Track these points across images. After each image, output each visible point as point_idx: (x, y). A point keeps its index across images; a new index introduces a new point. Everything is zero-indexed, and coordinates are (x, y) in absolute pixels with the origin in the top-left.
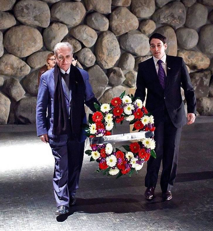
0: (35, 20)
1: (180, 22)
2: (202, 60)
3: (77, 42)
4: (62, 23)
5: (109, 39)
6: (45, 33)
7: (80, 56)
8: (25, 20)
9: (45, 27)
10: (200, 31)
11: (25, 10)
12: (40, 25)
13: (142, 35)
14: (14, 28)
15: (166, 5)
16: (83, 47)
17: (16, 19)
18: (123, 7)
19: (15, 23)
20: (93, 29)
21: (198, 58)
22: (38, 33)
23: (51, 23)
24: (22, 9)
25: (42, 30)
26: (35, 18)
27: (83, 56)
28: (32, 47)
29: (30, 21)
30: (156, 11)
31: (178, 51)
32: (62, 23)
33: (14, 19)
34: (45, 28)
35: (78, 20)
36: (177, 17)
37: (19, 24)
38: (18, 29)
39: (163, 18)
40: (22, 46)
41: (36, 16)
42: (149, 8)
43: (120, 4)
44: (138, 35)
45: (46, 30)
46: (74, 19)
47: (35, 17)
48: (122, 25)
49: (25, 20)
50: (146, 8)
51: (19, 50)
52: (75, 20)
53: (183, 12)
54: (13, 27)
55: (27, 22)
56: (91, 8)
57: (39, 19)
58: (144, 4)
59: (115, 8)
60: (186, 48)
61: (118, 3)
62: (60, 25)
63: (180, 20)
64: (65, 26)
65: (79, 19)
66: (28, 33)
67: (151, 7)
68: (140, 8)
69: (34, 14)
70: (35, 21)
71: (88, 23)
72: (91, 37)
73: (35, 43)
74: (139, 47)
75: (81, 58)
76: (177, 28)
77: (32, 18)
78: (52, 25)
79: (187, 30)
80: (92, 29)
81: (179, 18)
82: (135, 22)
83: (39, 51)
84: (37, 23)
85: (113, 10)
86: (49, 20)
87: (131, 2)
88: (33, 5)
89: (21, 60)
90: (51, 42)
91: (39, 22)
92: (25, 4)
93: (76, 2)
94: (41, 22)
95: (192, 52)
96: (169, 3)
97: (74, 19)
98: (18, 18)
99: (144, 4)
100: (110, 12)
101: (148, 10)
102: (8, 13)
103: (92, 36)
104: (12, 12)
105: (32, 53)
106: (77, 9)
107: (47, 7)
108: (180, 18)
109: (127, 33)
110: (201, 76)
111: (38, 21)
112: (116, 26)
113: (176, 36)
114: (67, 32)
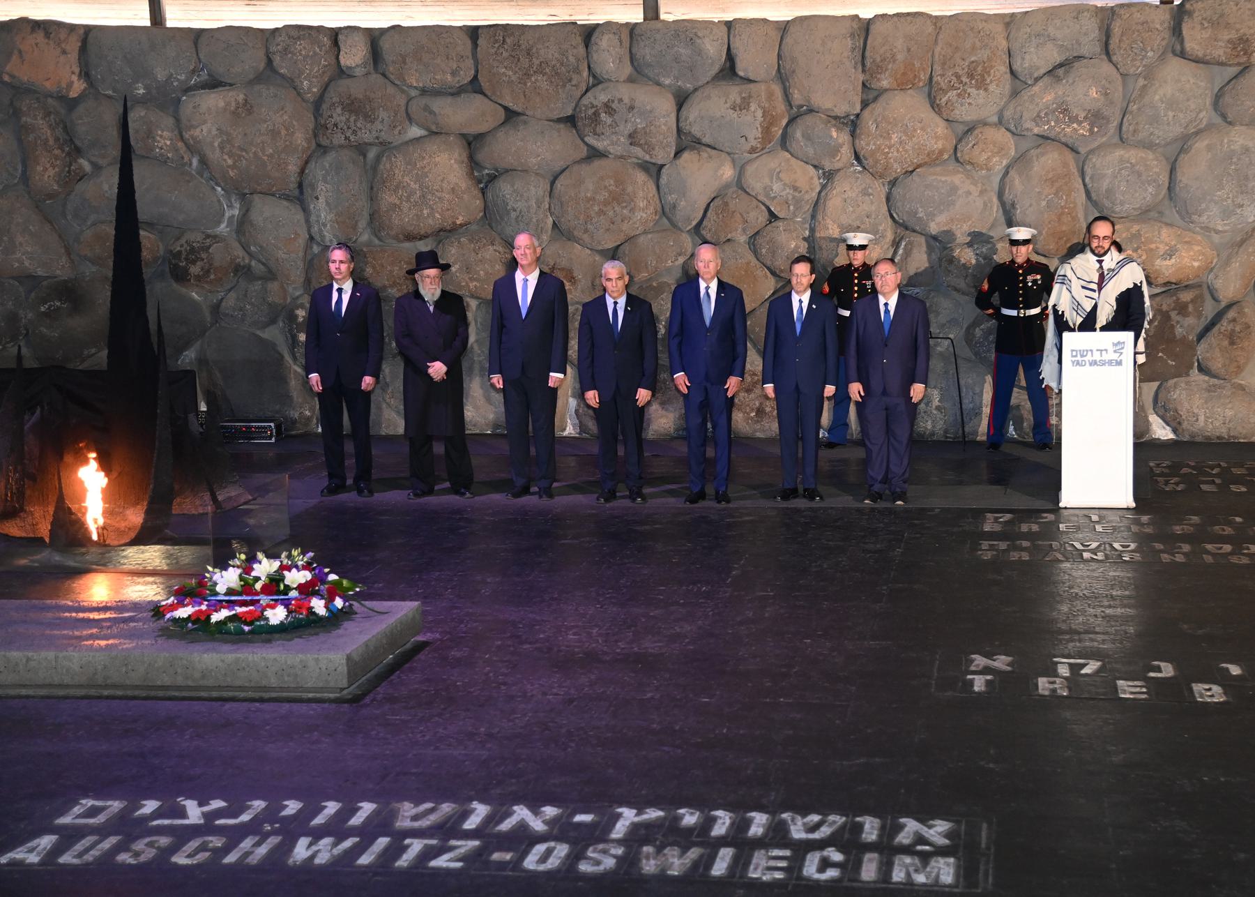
1: (1091, 131)
2: (1170, 254)
4: (709, 146)
5: (849, 194)
6: (664, 179)
12: (647, 158)
13: (957, 179)
14: (576, 167)
16: (773, 217)
21: (1153, 246)
22: (641, 177)
23: (678, 154)
24: (596, 114)
25: (654, 171)
26: (633, 138)
30: (1015, 93)
32: (709, 146)
34: (662, 166)
36: (1082, 115)
37: (595, 154)
38: (585, 169)
39: (1034, 120)
41: (635, 131)
42: (986, 90)
43: (885, 83)
45: (664, 170)
47: (630, 136)
48: (890, 148)
50: (973, 91)
51: (586, 231)
58: (964, 79)
59: (870, 95)
61: (879, 80)
63: (1092, 125)
64: (724, 155)
67: (992, 87)
69: (629, 128)
72: (796, 189)
73: (632, 210)
75: (764, 251)
77: (622, 139)
82: (935, 135)
83: (645, 232)
85: (865, 104)
86: (674, 144)
88: (626, 100)
92: (603, 98)
93: (752, 86)
94: (649, 148)
96: (1061, 65)
98: (586, 139)
99: (964, 79)
101: (977, 96)
102: (562, 126)
103: (798, 184)
104: (571, 121)
105: (622, 238)
106: (753, 107)
107: (664, 106)
108: (1096, 118)
110: (1165, 308)
111: (640, 145)
112: (873, 153)
113: (1083, 174)
114: (728, 172)
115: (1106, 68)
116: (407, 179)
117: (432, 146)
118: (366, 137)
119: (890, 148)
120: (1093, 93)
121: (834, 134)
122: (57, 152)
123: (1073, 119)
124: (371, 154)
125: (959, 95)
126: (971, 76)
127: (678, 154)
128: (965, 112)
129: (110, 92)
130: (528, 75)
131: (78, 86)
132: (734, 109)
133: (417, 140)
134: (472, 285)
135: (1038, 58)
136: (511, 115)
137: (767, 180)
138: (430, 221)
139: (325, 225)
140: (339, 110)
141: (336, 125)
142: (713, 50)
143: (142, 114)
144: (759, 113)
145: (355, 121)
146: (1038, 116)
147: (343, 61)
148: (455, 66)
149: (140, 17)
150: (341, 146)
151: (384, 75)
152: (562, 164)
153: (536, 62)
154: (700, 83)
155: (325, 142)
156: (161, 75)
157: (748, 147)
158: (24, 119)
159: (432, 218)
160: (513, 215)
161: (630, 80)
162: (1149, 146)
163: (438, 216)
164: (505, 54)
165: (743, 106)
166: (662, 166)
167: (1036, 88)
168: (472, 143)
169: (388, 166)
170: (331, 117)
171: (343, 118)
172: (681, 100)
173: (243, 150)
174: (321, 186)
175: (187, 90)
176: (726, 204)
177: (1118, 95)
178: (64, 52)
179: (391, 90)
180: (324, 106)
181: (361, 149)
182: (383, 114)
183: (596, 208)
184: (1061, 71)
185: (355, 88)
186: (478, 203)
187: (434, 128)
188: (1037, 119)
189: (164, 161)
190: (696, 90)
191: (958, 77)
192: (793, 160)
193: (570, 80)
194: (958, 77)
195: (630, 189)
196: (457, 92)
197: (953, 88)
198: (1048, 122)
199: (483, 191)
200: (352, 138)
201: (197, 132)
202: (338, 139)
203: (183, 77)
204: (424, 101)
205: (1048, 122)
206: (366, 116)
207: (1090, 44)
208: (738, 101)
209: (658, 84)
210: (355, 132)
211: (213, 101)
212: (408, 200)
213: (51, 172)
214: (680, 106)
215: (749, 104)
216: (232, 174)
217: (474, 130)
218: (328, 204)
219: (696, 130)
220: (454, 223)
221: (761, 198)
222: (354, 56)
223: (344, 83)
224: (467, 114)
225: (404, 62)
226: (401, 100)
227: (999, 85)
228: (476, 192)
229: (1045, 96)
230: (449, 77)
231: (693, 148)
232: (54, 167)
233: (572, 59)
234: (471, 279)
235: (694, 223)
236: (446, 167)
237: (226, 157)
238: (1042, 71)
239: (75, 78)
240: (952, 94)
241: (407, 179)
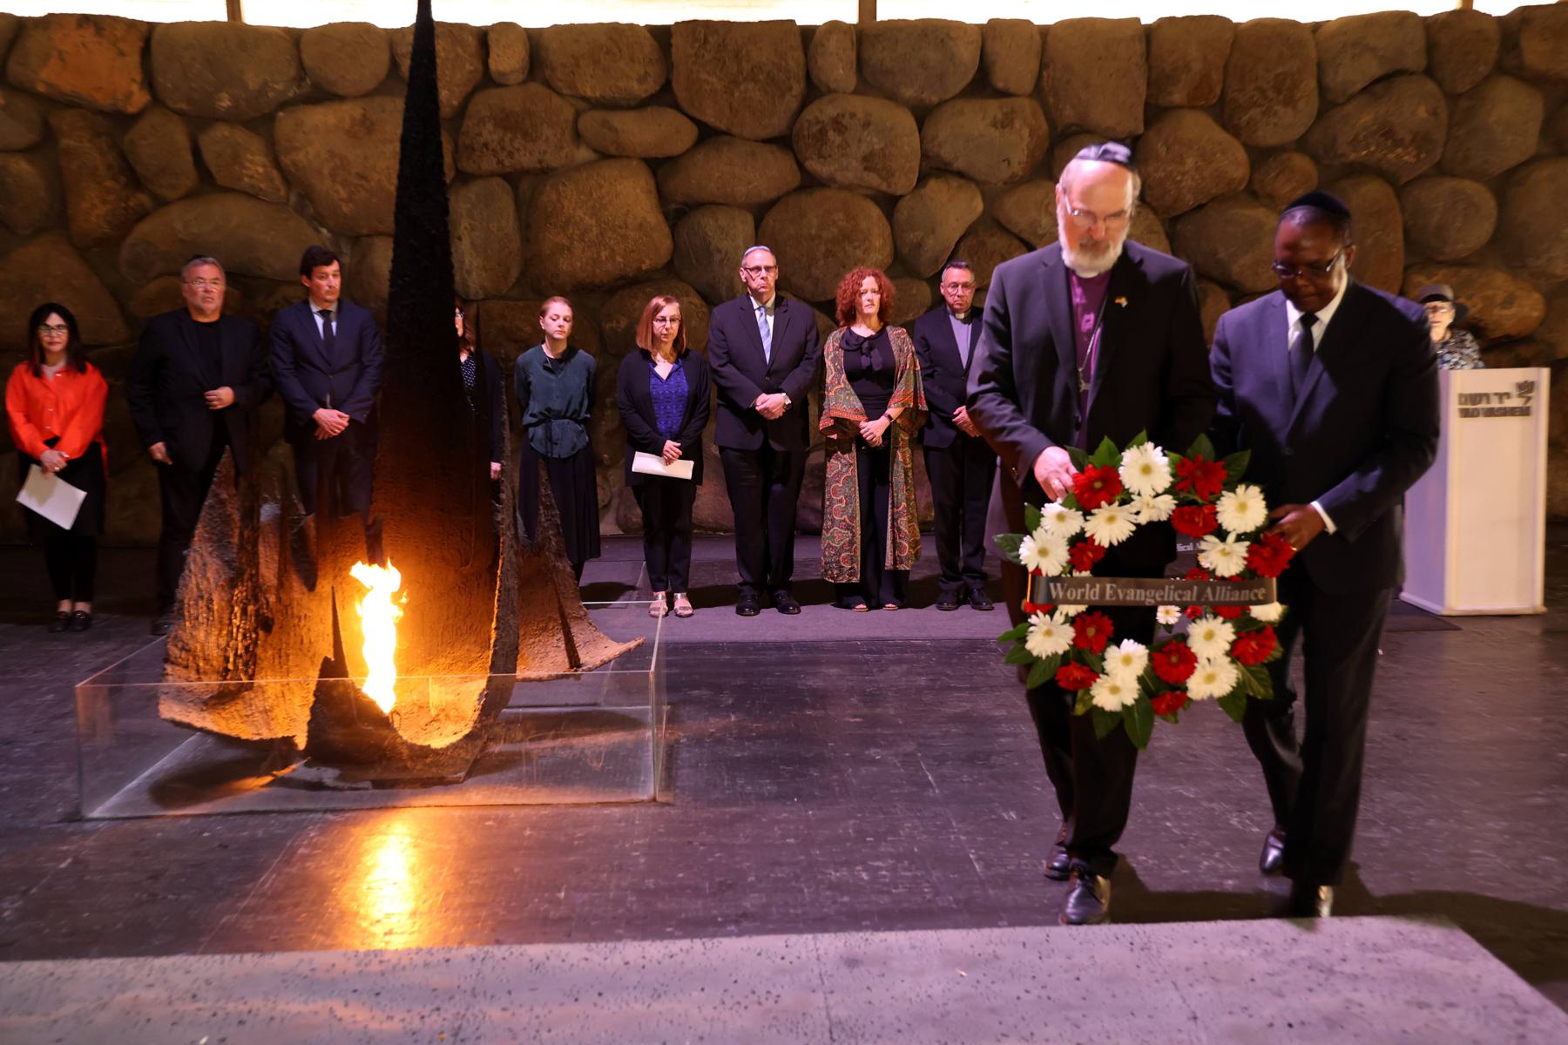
1: (1417, 156)
2: (1508, 302)
3: (1016, 243)
4: (961, 175)
9: (899, 193)
10: (1505, 184)
11: (831, 134)
12: (884, 187)
15: (1364, 90)
17: (800, 166)
18: (1193, 108)
19: (794, 179)
21: (1490, 292)
22: (875, 212)
23: (922, 180)
24: (823, 131)
25: (889, 203)
26: (868, 162)
30: (1321, 115)
31: (1406, 268)
32: (961, 175)
33: (795, 167)
36: (1408, 138)
37: (810, 183)
43: (1178, 97)
44: (1247, 212)
45: (902, 203)
47: (865, 159)
53: (1434, 113)
54: (788, 194)
55: (839, 176)
56: (1068, 114)
58: (1271, 94)
59: (1155, 113)
60: (1441, 258)
62: (955, 182)
65: (1024, 159)
66: (841, 216)
67: (1301, 105)
68: (1258, 110)
69: (864, 149)
70: (866, 174)
73: (866, 251)
74: (1246, 260)
76: (1404, 180)
77: (854, 163)
79: (1449, 184)
81: (1413, 141)
82: (1234, 162)
84: (873, 179)
85: (1149, 122)
87: (1223, 91)
88: (860, 115)
89: (817, 313)
90: (919, 245)
95: (1465, 272)
99: (1271, 94)
100: (1141, 130)
102: (774, 148)
104: (783, 142)
106: (1017, 124)
107: (907, 121)
108: (1421, 140)
109: (1201, 207)
114: (978, 206)
115: (1431, 86)
116: (580, 213)
117: (609, 170)
118: (526, 159)
119: (1184, 174)
120: (1422, 112)
122: (109, 184)
123: (1398, 143)
124: (525, 186)
125: (1264, 113)
126: (1279, 92)
127: (922, 180)
128: (1268, 135)
129: (183, 106)
130: (735, 82)
131: (140, 99)
132: (994, 125)
133: (589, 164)
135: (1354, 73)
136: (707, 135)
138: (609, 266)
139: (469, 272)
140: (490, 126)
141: (486, 145)
142: (968, 56)
143: (226, 133)
144: (1026, 132)
145: (512, 140)
146: (1355, 139)
147: (494, 64)
148: (642, 72)
149: (221, 15)
150: (492, 175)
151: (548, 84)
152: (773, 194)
153: (746, 67)
154: (949, 96)
155: (468, 166)
156: (253, 82)
158: (65, 142)
159: (613, 262)
160: (717, 257)
161: (856, 92)
162: (1477, 176)
163: (619, 259)
164: (708, 57)
165: (1005, 123)
167: (1349, 108)
168: (659, 167)
169: (554, 197)
170: (480, 135)
171: (495, 137)
172: (923, 115)
173: (364, 178)
174: (465, 223)
175: (285, 105)
177: (1444, 116)
178: (121, 54)
179: (556, 100)
180: (469, 123)
181: (512, 178)
182: (547, 131)
183: (823, 248)
184: (1379, 88)
185: (511, 99)
186: (668, 243)
187: (613, 151)
188: (1354, 143)
189: (252, 195)
190: (941, 104)
191: (1262, 91)
193: (790, 89)
194: (1262, 91)
195: (864, 225)
196: (642, 104)
197: (1255, 105)
198: (1367, 147)
199: (673, 228)
200: (507, 163)
201: (300, 157)
202: (489, 164)
203: (280, 87)
204: (597, 115)
205: (1367, 147)
206: (527, 136)
207: (1414, 59)
208: (1000, 116)
209: (893, 97)
210: (511, 154)
211: (319, 116)
212: (582, 240)
213: (102, 210)
214: (921, 121)
215: (1012, 121)
216: (345, 209)
217: (658, 153)
218: (473, 243)
219: (947, 153)
220: (639, 269)
221: (1025, 236)
222: (507, 61)
223: (492, 96)
224: (661, 131)
225: (577, 65)
226: (568, 113)
227: (1308, 104)
228: (667, 230)
229: (1366, 117)
230: (636, 85)
231: (938, 177)
232: (104, 202)
233: (792, 64)
236: (632, 196)
237: (338, 187)
238: (1359, 86)
239: (135, 88)
240: (1255, 112)
241: (580, 213)
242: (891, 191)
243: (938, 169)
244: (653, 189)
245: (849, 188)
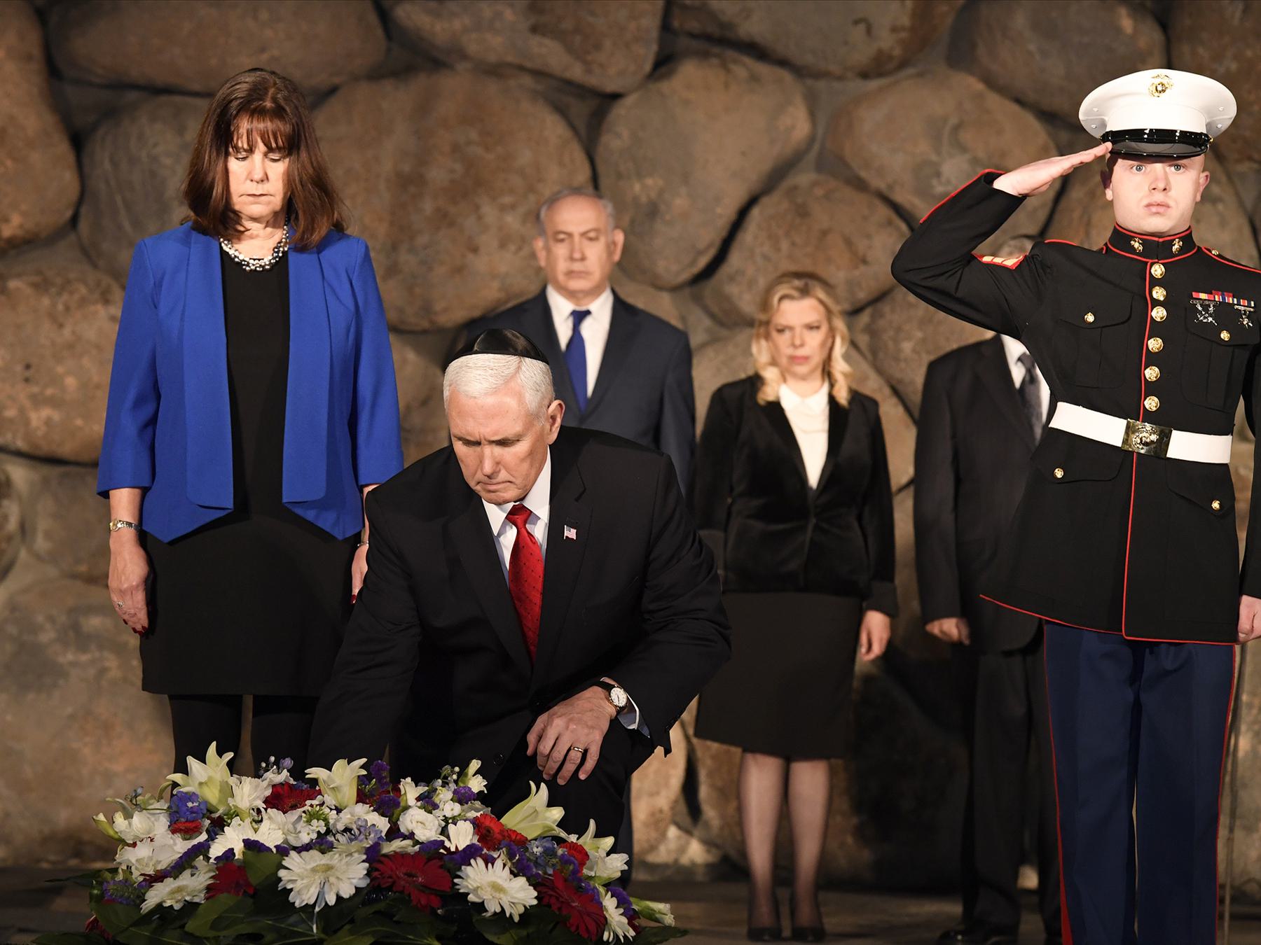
0: (534, 29)
3: (883, 211)
7: (899, 329)
8: (457, 24)
9: (610, 87)
12: (576, 72)
20: (1019, 101)
22: (554, 129)
27: (919, 334)
28: (503, 245)
29: (496, 41)
33: (373, 18)
34: (616, 97)
35: (894, 29)
40: (422, 240)
46: (862, 27)
49: (457, 24)
52: (869, 31)
55: (472, 48)
57: (567, 25)
71: (981, 51)
75: (907, 346)
78: (668, 75)
80: (1015, 108)
84: (550, 54)
91: (570, 49)
97: (856, 22)
114: (797, 124)
121: (1127, 24)
134: (38, 418)
137: (924, 148)
157: (862, 54)
166: (616, 97)
176: (803, 212)
183: (428, 206)
186: (68, 178)
192: (994, 101)
195: (525, 157)
228: (63, 148)
231: (704, 55)
234: (38, 401)
235: (703, 262)
242: (593, 81)
243: (708, 38)
244: (37, 52)
245: (496, 71)
